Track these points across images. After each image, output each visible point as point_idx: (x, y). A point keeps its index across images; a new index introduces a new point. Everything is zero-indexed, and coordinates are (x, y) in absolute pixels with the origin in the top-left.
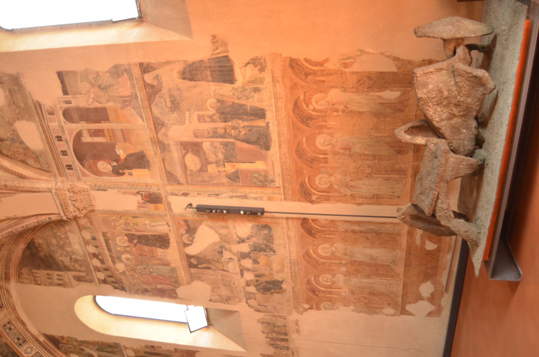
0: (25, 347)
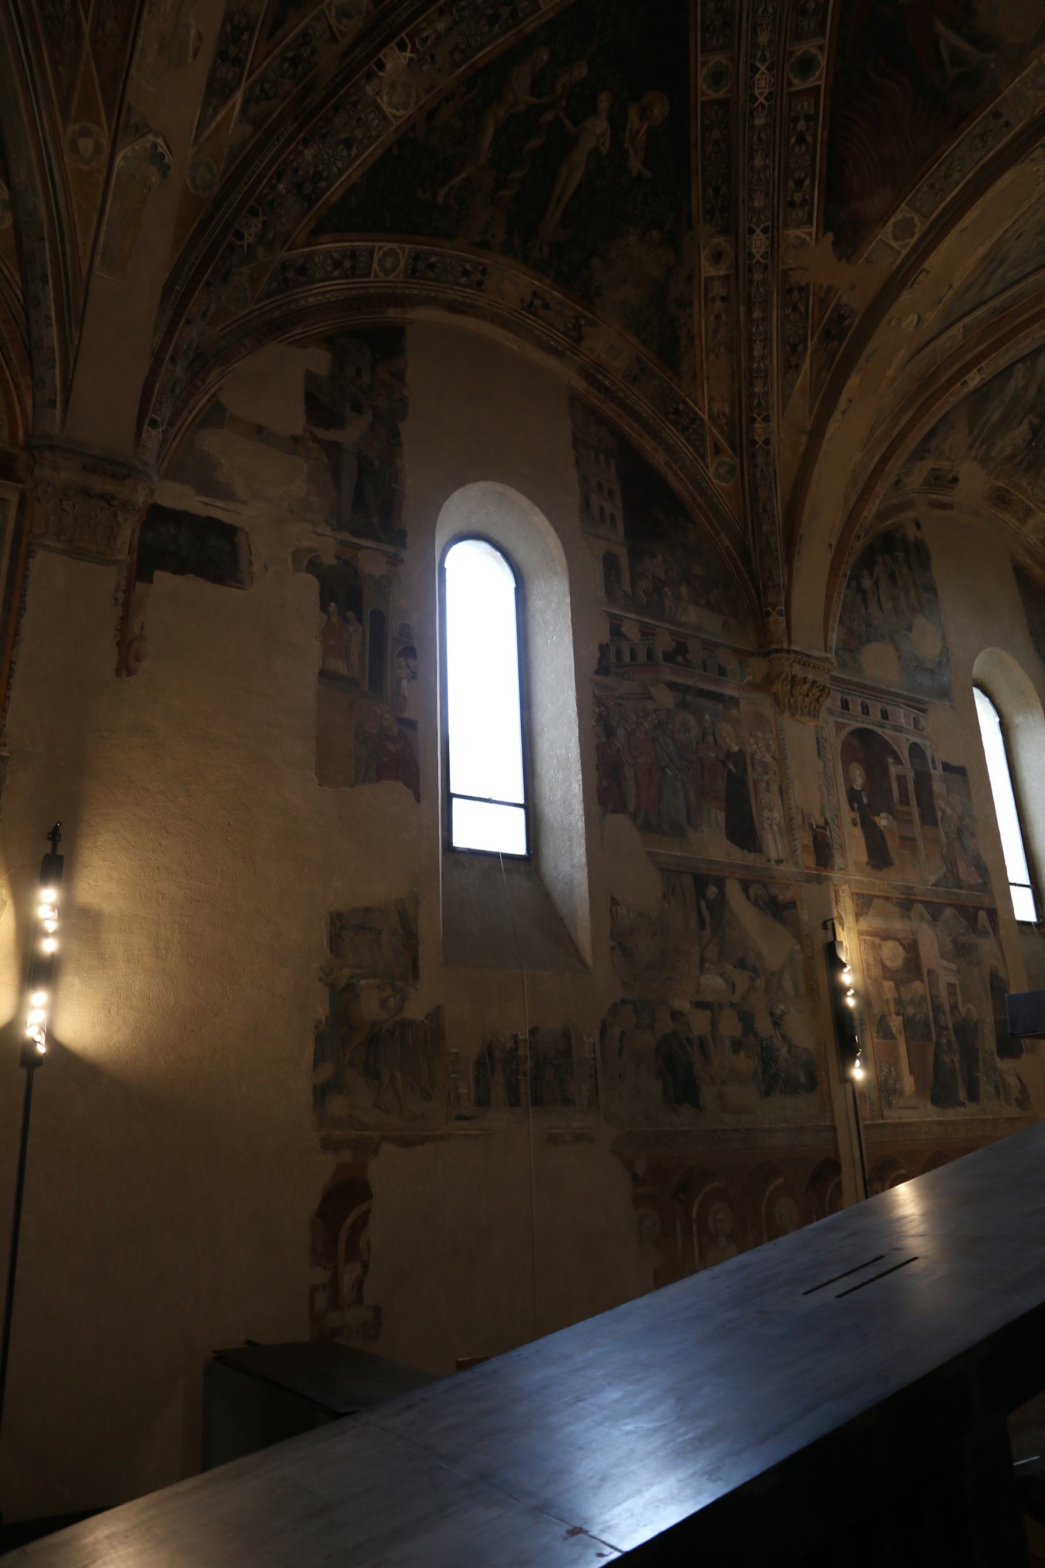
0: (402, 262)
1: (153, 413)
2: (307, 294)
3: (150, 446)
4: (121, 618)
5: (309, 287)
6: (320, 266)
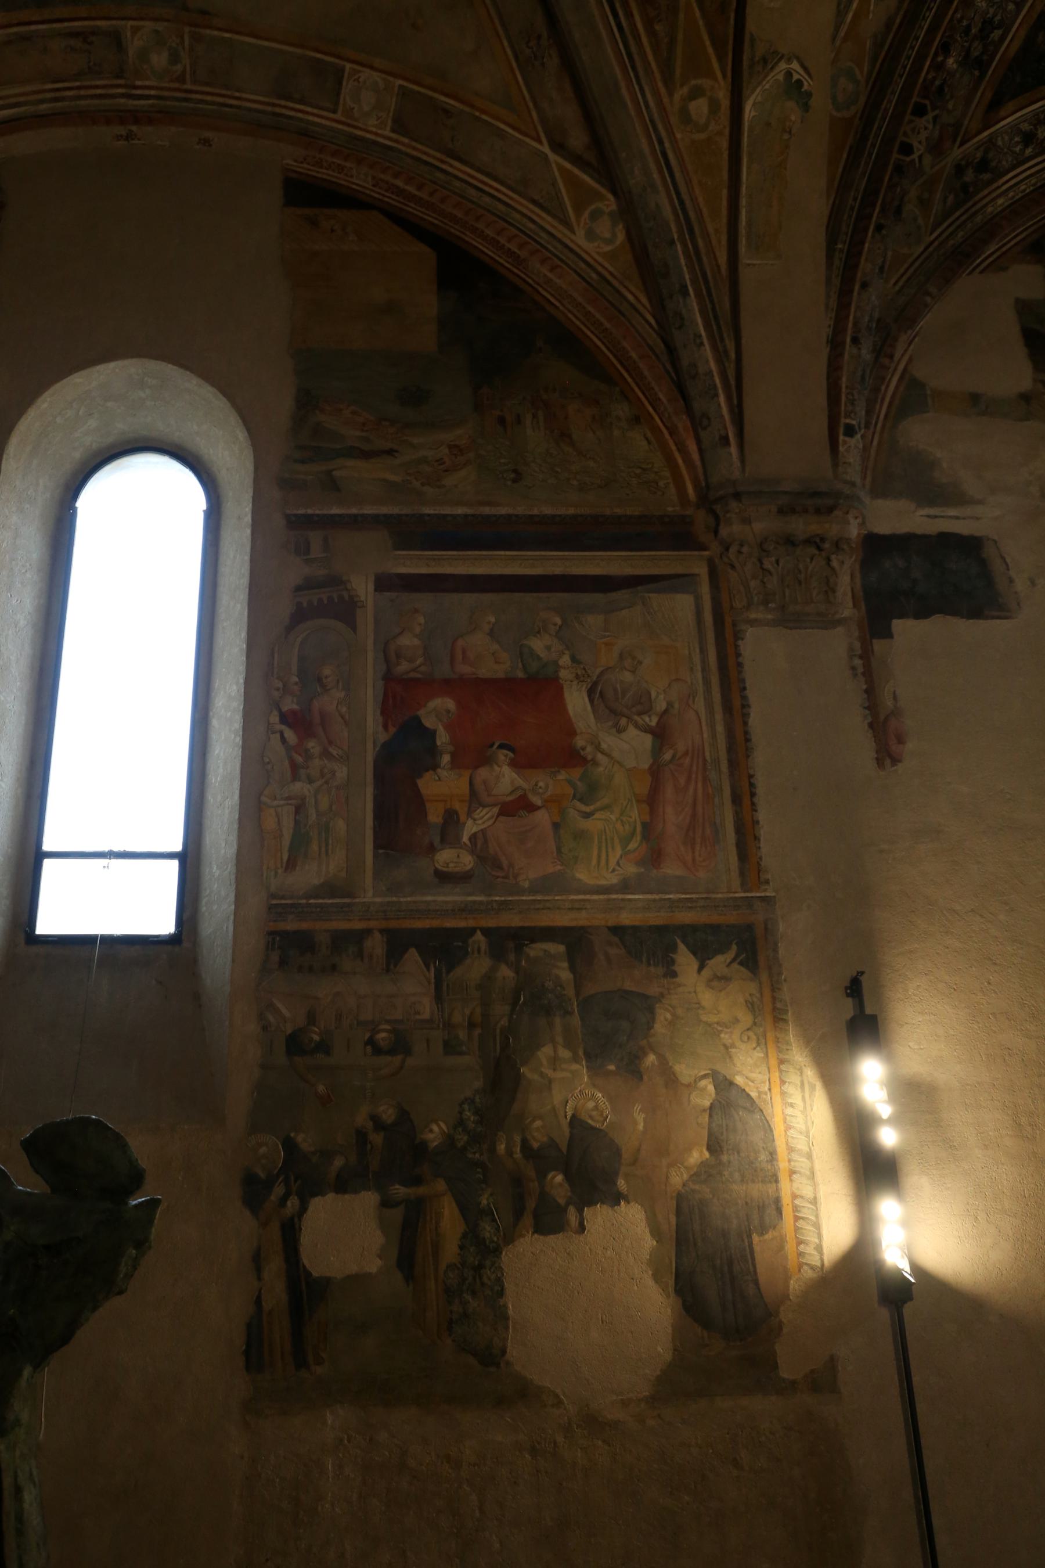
1: (845, 418)
2: (994, 195)
3: (852, 460)
4: (866, 691)
5: (995, 185)
6: (1005, 150)
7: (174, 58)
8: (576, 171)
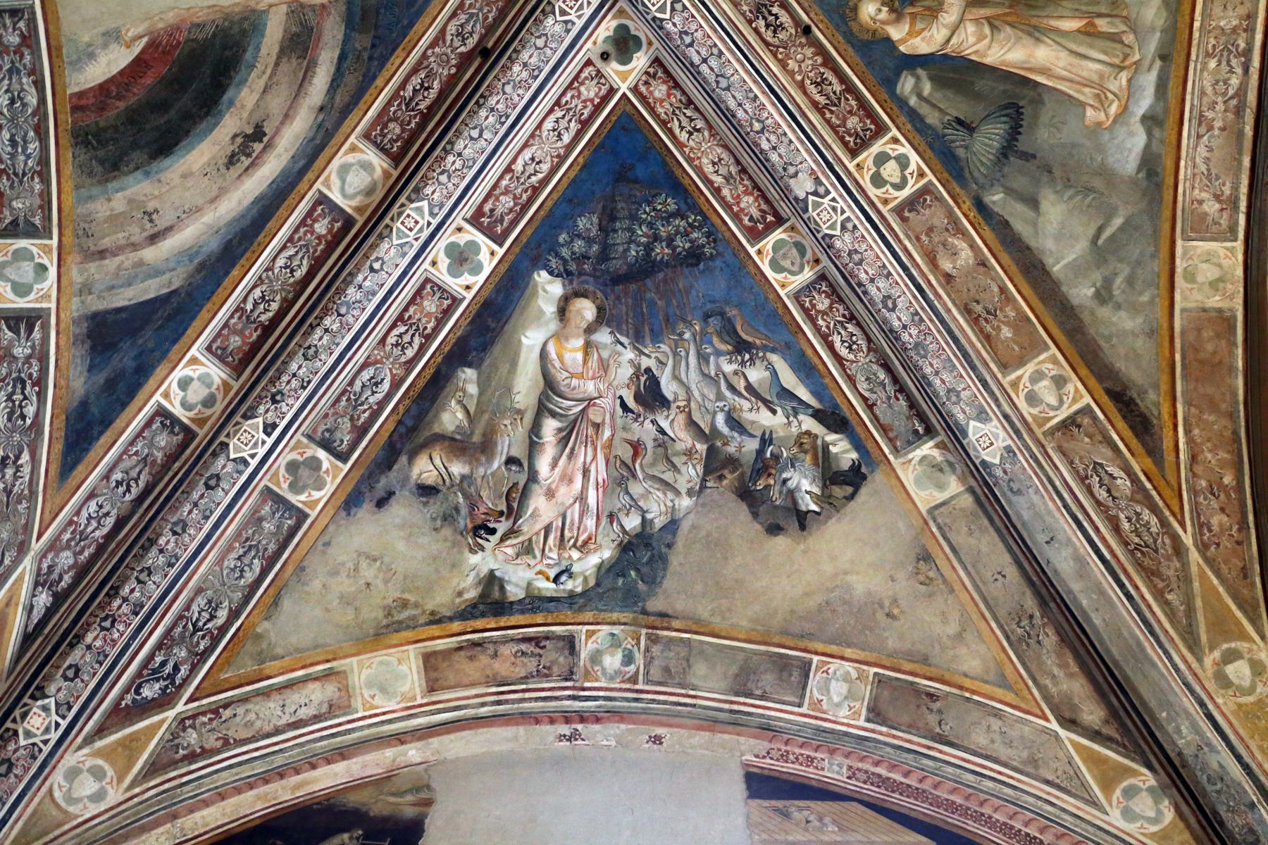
7: (628, 659)
8: (1096, 747)
